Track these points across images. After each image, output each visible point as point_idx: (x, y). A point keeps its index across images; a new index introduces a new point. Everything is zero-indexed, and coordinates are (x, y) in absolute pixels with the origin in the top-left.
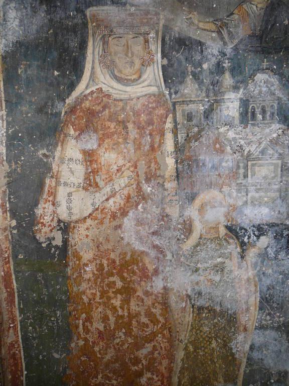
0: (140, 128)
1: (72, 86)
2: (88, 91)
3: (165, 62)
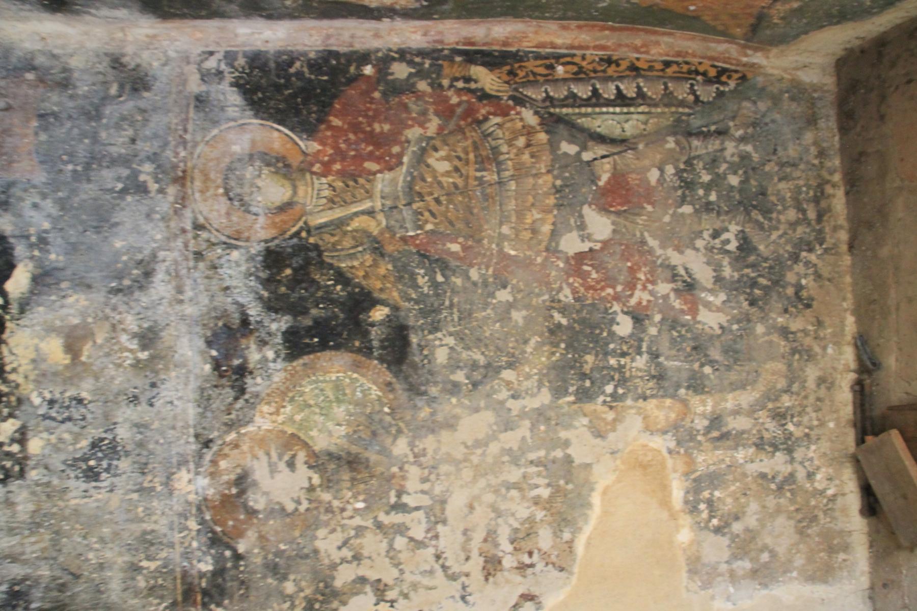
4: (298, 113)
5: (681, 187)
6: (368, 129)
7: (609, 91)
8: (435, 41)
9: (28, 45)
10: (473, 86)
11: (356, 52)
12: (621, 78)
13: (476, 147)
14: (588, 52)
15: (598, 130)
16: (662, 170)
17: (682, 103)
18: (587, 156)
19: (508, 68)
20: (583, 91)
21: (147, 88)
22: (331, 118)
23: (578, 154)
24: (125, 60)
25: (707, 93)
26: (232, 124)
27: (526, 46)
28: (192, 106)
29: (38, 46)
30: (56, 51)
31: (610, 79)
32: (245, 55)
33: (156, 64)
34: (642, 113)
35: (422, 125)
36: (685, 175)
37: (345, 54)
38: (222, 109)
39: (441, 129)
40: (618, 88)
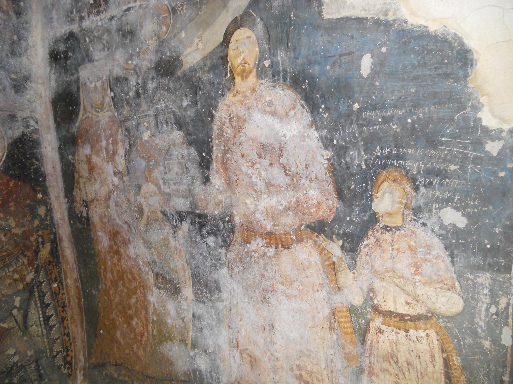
0: (107, 140)
1: (77, 115)
2: (84, 118)
3: (112, 94)
4: (14, 165)
5: (7, 369)
6: (10, 200)
7: (50, 312)
8: (58, 224)
9: (30, 39)
10: (41, 246)
11: (47, 189)
12: (57, 315)
13: (9, 255)
14: (66, 295)
15: (30, 313)
16: (15, 354)
17: (51, 350)
18: (15, 312)
19: (52, 261)
20: (47, 299)
21: (16, 92)
22: (13, 181)
23: (15, 307)
24: (28, 82)
25: (59, 361)
26: (3, 133)
27: (63, 266)
28: (10, 113)
29: (30, 44)
30: (28, 51)
31: (56, 311)
32: (38, 138)
33: (28, 97)
34: (42, 332)
35: (17, 226)
36: (15, 368)
37: (45, 184)
38: (10, 128)
39: (16, 235)
40: (52, 315)
